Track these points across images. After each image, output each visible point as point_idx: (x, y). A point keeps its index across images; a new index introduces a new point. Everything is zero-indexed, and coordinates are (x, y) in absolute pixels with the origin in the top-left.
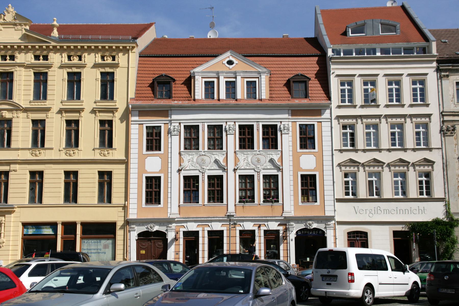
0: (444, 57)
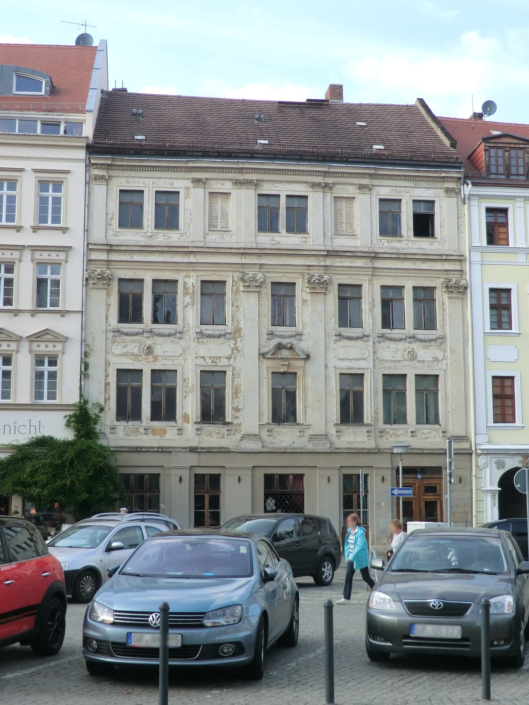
0: (105, 144)
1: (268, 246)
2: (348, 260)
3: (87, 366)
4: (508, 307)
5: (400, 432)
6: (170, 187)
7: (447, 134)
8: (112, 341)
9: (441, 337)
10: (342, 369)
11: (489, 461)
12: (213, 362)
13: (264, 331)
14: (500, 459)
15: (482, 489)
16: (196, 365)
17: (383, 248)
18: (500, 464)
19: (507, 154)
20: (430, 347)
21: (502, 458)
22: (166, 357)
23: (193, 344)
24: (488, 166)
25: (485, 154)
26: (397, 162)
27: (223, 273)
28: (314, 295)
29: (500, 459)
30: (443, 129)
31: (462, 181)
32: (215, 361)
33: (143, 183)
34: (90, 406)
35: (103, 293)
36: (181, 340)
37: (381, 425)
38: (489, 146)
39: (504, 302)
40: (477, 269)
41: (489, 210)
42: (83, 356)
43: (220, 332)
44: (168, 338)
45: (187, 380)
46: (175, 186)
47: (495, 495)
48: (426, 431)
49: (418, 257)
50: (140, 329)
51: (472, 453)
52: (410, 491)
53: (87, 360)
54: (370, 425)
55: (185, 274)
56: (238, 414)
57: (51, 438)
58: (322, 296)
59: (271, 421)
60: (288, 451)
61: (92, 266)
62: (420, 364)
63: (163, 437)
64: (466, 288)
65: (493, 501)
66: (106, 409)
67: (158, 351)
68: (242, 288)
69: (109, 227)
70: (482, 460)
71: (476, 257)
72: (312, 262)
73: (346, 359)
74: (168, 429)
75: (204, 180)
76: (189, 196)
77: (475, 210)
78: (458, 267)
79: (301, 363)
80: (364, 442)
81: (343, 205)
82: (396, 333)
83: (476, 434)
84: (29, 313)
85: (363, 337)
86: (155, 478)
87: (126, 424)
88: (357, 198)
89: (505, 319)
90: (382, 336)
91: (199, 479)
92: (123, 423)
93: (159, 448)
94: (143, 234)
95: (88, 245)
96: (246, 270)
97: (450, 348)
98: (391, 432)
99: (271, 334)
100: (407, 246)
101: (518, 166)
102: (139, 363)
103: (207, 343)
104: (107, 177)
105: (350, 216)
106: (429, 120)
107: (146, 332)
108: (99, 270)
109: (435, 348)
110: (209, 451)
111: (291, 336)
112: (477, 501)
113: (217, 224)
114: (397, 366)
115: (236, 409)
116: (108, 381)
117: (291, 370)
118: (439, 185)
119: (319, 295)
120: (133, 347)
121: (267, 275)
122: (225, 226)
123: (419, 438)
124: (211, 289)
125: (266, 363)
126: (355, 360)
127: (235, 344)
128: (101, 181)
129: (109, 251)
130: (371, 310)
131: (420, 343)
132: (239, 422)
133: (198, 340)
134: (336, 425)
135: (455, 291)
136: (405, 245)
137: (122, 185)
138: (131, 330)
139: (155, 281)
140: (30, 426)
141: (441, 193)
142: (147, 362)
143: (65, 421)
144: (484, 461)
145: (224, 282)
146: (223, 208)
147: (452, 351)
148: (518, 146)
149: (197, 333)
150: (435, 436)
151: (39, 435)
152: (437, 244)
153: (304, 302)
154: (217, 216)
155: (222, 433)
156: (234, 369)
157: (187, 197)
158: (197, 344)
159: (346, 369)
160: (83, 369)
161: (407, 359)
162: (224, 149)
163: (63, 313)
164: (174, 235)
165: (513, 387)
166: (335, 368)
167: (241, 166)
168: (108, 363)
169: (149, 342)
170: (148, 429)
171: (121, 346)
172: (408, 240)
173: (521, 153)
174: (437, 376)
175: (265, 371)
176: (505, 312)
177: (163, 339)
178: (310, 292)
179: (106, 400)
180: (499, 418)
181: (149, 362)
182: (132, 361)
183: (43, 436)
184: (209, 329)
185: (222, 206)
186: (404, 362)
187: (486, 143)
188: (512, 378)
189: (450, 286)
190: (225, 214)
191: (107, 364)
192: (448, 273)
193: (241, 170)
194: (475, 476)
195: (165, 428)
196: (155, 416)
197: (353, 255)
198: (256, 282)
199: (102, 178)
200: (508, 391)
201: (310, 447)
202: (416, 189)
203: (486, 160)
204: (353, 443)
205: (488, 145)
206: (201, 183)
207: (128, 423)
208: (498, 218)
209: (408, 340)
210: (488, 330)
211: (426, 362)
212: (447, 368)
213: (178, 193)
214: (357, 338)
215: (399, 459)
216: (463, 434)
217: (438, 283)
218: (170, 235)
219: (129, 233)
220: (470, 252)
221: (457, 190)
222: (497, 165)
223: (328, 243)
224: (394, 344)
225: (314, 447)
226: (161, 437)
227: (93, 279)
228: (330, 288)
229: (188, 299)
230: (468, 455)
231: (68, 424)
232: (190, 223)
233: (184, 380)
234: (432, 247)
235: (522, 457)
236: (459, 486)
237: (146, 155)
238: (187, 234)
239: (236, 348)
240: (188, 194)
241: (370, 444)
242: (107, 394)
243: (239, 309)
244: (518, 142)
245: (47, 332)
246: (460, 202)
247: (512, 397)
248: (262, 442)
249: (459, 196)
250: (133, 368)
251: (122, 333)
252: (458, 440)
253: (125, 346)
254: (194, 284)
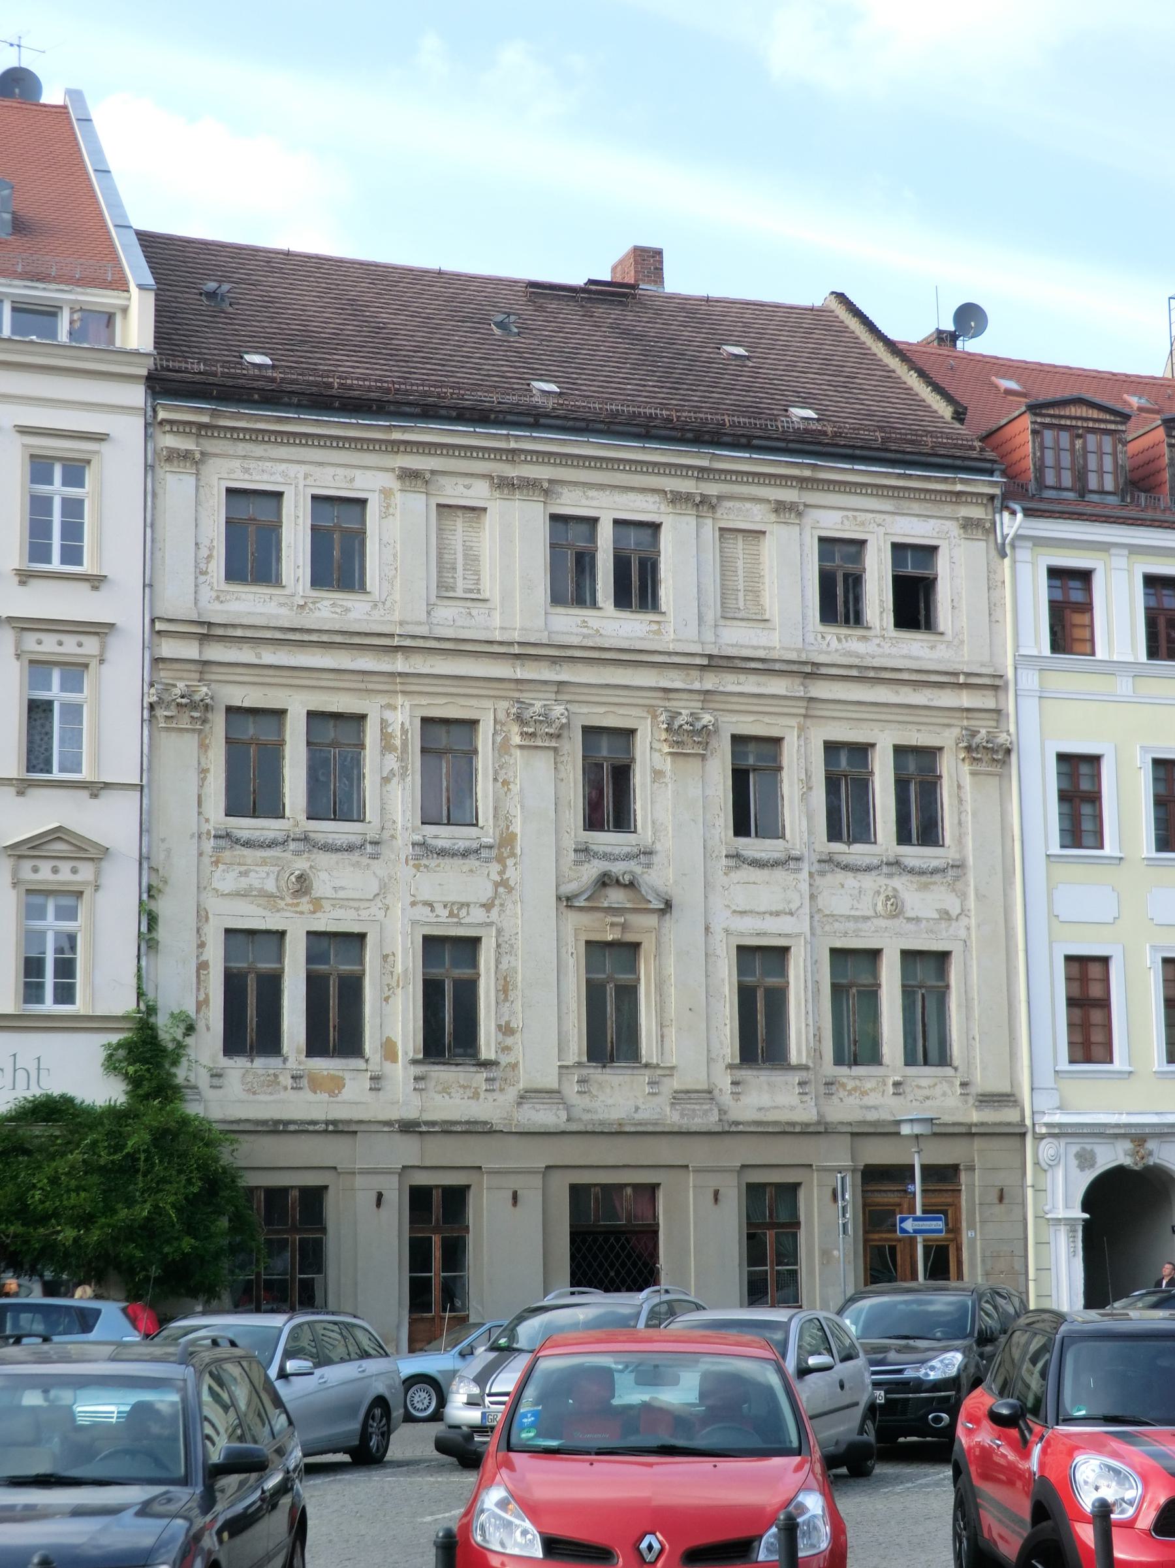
0: (186, 371)
1: (575, 641)
2: (753, 678)
3: (153, 920)
4: (1094, 798)
5: (869, 1085)
6: (345, 486)
7: (938, 389)
8: (213, 859)
9: (958, 863)
10: (742, 934)
11: (1062, 1150)
12: (451, 915)
13: (569, 844)
15: (1048, 1216)
16: (414, 923)
17: (828, 653)
18: (1086, 1160)
19: (1079, 443)
20: (932, 887)
21: (1089, 1144)
22: (341, 902)
23: (405, 872)
24: (1040, 469)
25: (1034, 442)
26: (858, 452)
27: (473, 702)
28: (680, 760)
30: (922, 374)
31: (997, 503)
32: (456, 912)
33: (284, 474)
34: (161, 1021)
35: (191, 741)
36: (376, 861)
37: (829, 1068)
38: (1040, 423)
39: (1085, 785)
40: (1030, 707)
41: (1055, 573)
42: (145, 896)
43: (467, 844)
44: (346, 855)
45: (391, 958)
46: (358, 484)
47: (1075, 1231)
48: (924, 1082)
49: (905, 676)
50: (278, 832)
51: (1023, 1135)
52: (940, 1223)
53: (153, 906)
54: (806, 1068)
55: (383, 700)
56: (509, 1041)
57: (67, 1101)
58: (696, 764)
59: (585, 1059)
60: (627, 1129)
61: (162, 674)
62: (911, 927)
63: (337, 1096)
64: (1008, 752)
65: (1072, 1245)
66: (200, 1026)
67: (322, 886)
68: (517, 740)
69: (202, 578)
70: (1048, 1149)
71: (1029, 680)
72: (674, 680)
73: (751, 912)
74: (347, 1076)
75: (428, 476)
76: (391, 510)
77: (1025, 571)
78: (991, 704)
79: (651, 920)
80: (792, 1108)
81: (739, 546)
82: (858, 852)
83: (1032, 1089)
84: (12, 785)
85: (788, 861)
86: (313, 1198)
87: (249, 1065)
88: (772, 533)
89: (1087, 825)
90: (829, 861)
91: (419, 1198)
92: (241, 1062)
93: (327, 1123)
94: (283, 600)
95: (153, 621)
96: (526, 697)
97: (976, 890)
98: (850, 1085)
99: (584, 852)
100: (881, 650)
101: (1101, 472)
102: (278, 915)
103: (438, 869)
104: (198, 456)
105: (754, 577)
106: (879, 349)
107: (293, 840)
108: (181, 685)
109: (943, 888)
110: (447, 1129)
111: (628, 857)
112: (1037, 1243)
113: (455, 583)
114: (860, 930)
115: (506, 1030)
116: (204, 958)
117: (630, 937)
118: (948, 510)
119: (691, 759)
120: (264, 875)
121: (574, 708)
122: (473, 587)
123: (910, 1097)
124: (442, 738)
125: (573, 919)
126: (771, 914)
127: (501, 873)
128: (182, 464)
129: (204, 638)
130: (804, 797)
131: (910, 877)
132: (513, 1061)
133: (416, 862)
134: (731, 1068)
135: (986, 758)
136: (876, 648)
137: (232, 476)
138: (258, 833)
139: (313, 716)
140: (15, 1070)
141: (953, 528)
142: (296, 912)
143: (102, 1055)
144: (1052, 1152)
145: (474, 723)
146: (467, 544)
147: (980, 897)
148: (1103, 426)
149: (414, 844)
150: (944, 1094)
151: (36, 1092)
152: (943, 647)
153: (657, 774)
154: (455, 563)
155: (474, 1085)
156: (499, 932)
157: (386, 514)
158: (414, 871)
159: (751, 935)
160: (144, 929)
161: (883, 913)
162: (467, 400)
163: (95, 789)
164: (357, 604)
165: (1106, 980)
166: (727, 931)
167: (513, 445)
168: (203, 913)
169: (301, 864)
170: (301, 1077)
171: (235, 874)
172: (883, 636)
173: (1107, 441)
174: (943, 957)
175: (571, 939)
176: (1086, 809)
177: (339, 856)
178: (670, 754)
179: (201, 1005)
180: (1079, 1054)
181: (302, 913)
182: (260, 909)
183: (47, 1095)
184: (442, 835)
185: (466, 538)
186: (875, 921)
187: (1036, 415)
188: (1105, 961)
189: (974, 745)
190: (472, 559)
191: (202, 915)
192: (970, 715)
193: (512, 455)
194: (1033, 1186)
195: (340, 1073)
196: (316, 1045)
197: (765, 667)
198: (550, 724)
199: (186, 456)
200: (1095, 991)
201: (673, 1118)
202: (898, 518)
203: (1034, 454)
204: (768, 1109)
205: (1039, 420)
206: (419, 482)
207: (252, 1061)
208: (1071, 591)
209: (885, 869)
210: (1056, 849)
211: (924, 922)
212: (969, 935)
213: (363, 502)
214: (776, 864)
215: (913, 1150)
216: (1005, 1088)
217: (946, 738)
218: (349, 604)
219: (251, 597)
221: (988, 525)
222: (1058, 468)
223: (709, 636)
224: (855, 877)
225: (685, 1120)
226: (330, 1096)
227: (167, 707)
228: (714, 743)
229: (391, 762)
230: (1018, 1139)
231: (111, 1065)
232: (395, 577)
233: (385, 957)
234: (935, 655)
235: (1132, 1141)
236: (998, 1209)
237: (288, 406)
238: (388, 604)
239: (504, 883)
240: (388, 507)
241: (806, 1113)
242: (202, 990)
243: (509, 789)
244: (1102, 416)
245: (58, 834)
246: (993, 553)
247: (1104, 1004)
248: (568, 1108)
249: (992, 537)
250: (263, 927)
251: (237, 841)
252: (994, 1102)
253: (244, 874)
254: (407, 725)
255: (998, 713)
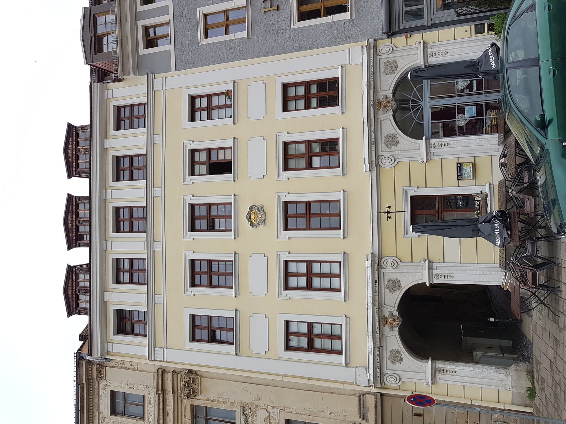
14: (388, 356)
21: (387, 354)
29: (388, 356)
70: (390, 382)
78: (170, 375)
141: (103, 383)
202: (101, 411)
216: (357, 399)
220: (155, 360)
234: (152, 400)
235: (384, 326)
255: (174, 372)
